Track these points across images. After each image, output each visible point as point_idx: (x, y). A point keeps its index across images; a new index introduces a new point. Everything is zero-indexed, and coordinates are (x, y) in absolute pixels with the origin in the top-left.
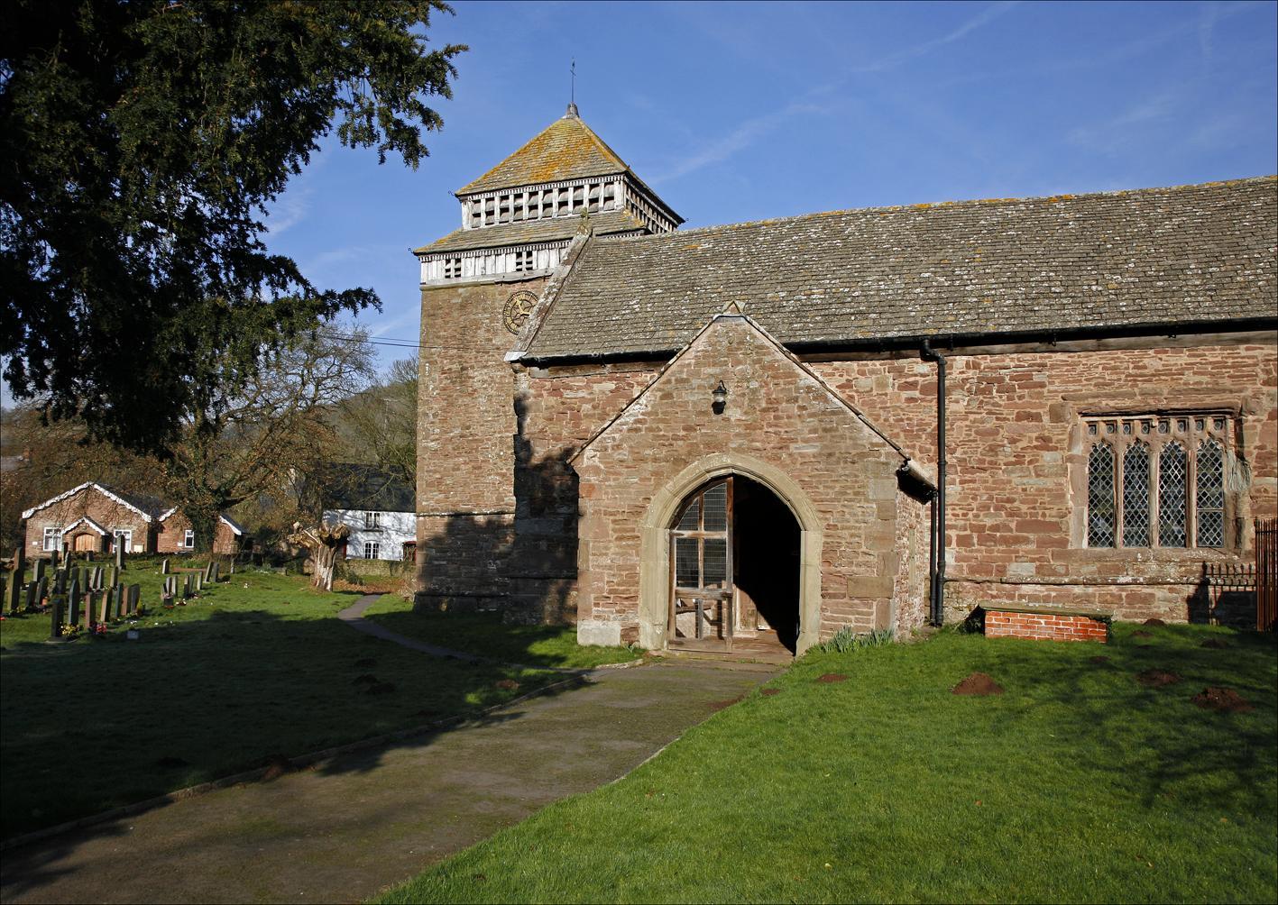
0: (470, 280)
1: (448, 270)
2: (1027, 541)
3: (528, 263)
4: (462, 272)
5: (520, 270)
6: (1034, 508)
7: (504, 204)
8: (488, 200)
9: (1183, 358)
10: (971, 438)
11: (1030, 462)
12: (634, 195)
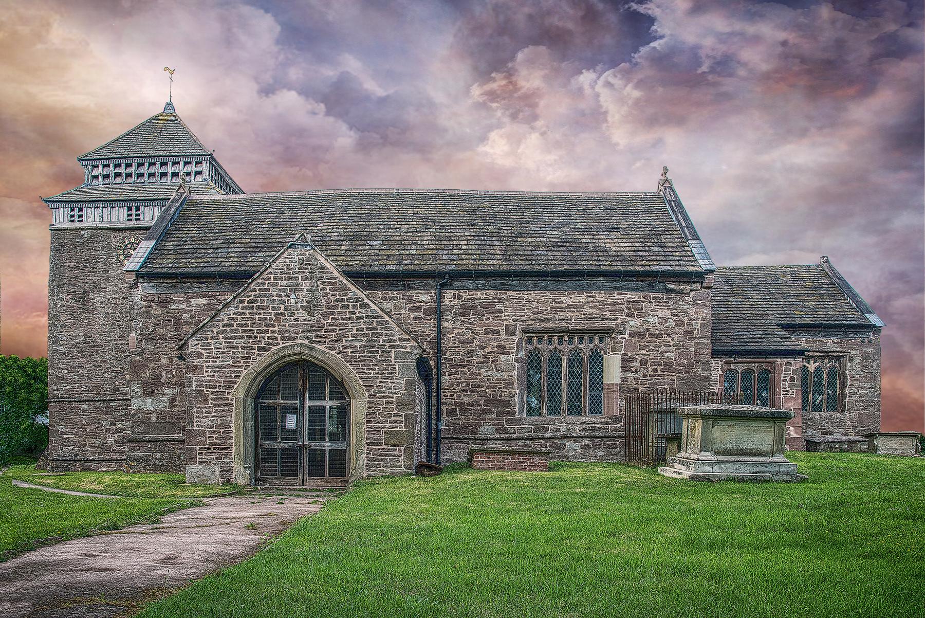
1: (72, 216)
2: (490, 411)
3: (136, 215)
4: (84, 218)
5: (131, 220)
6: (495, 391)
7: (117, 170)
8: (104, 166)
9: (583, 298)
10: (456, 345)
11: (493, 362)
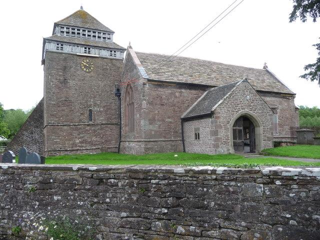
0: (66, 52)
7: (79, 32)
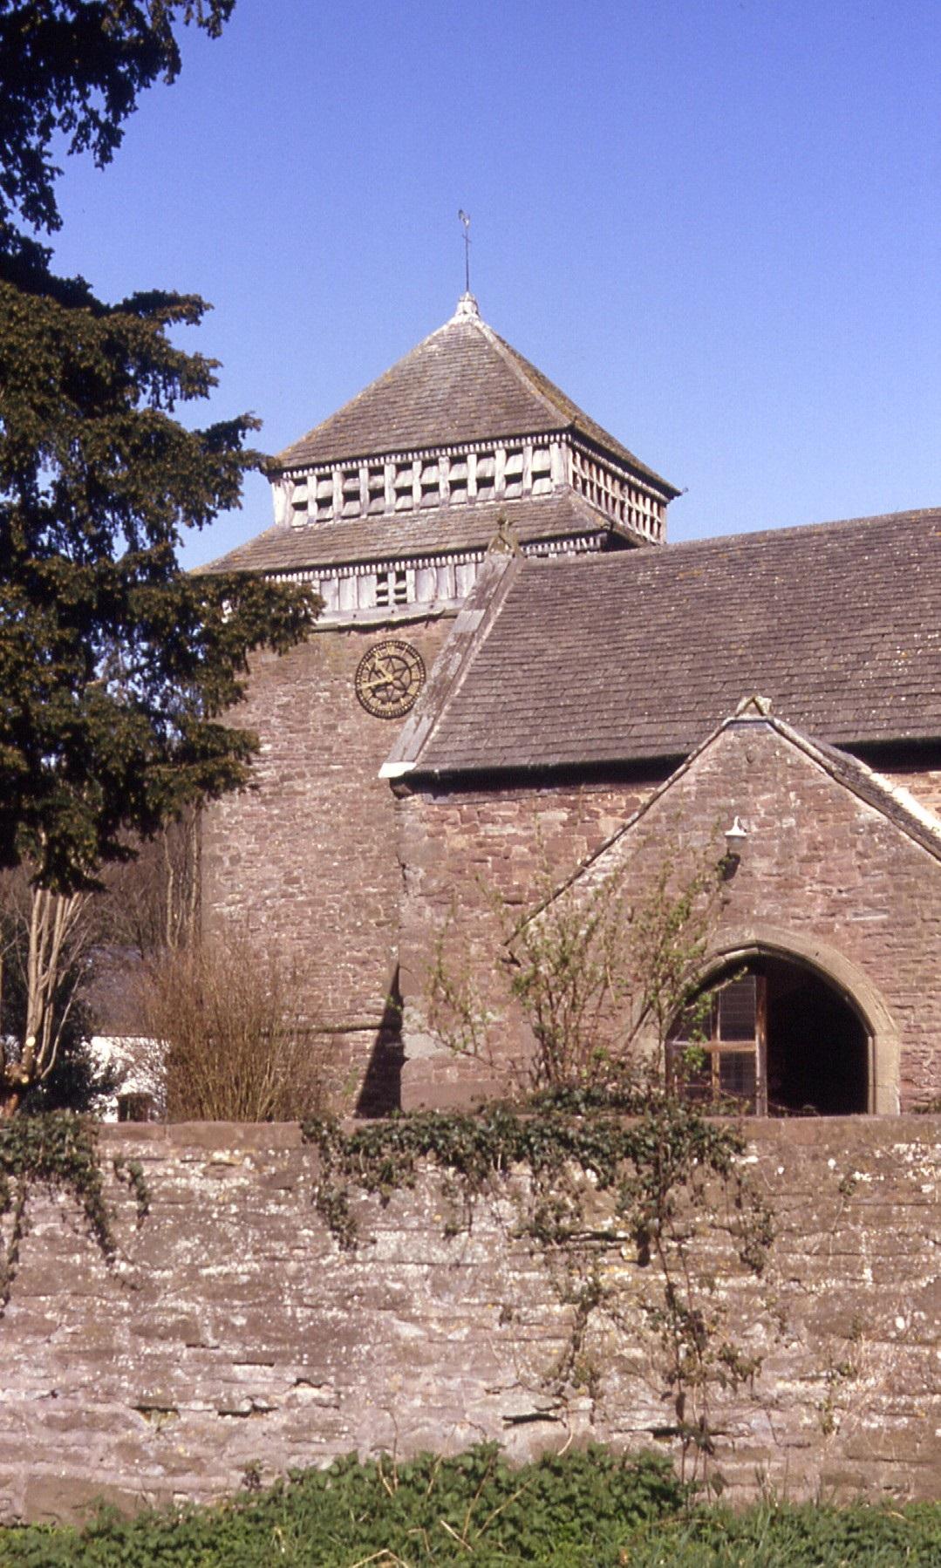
3: (398, 592)
5: (385, 604)
7: (350, 485)
12: (586, 463)
